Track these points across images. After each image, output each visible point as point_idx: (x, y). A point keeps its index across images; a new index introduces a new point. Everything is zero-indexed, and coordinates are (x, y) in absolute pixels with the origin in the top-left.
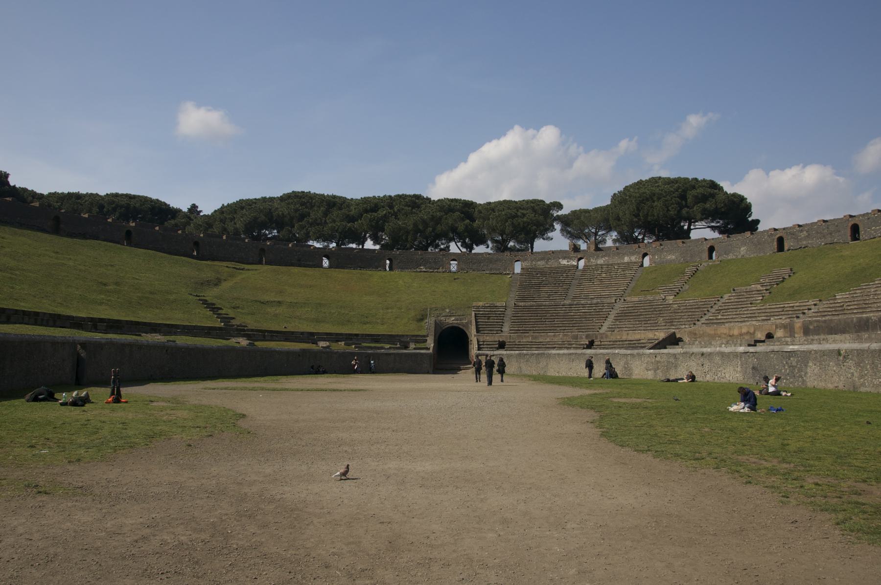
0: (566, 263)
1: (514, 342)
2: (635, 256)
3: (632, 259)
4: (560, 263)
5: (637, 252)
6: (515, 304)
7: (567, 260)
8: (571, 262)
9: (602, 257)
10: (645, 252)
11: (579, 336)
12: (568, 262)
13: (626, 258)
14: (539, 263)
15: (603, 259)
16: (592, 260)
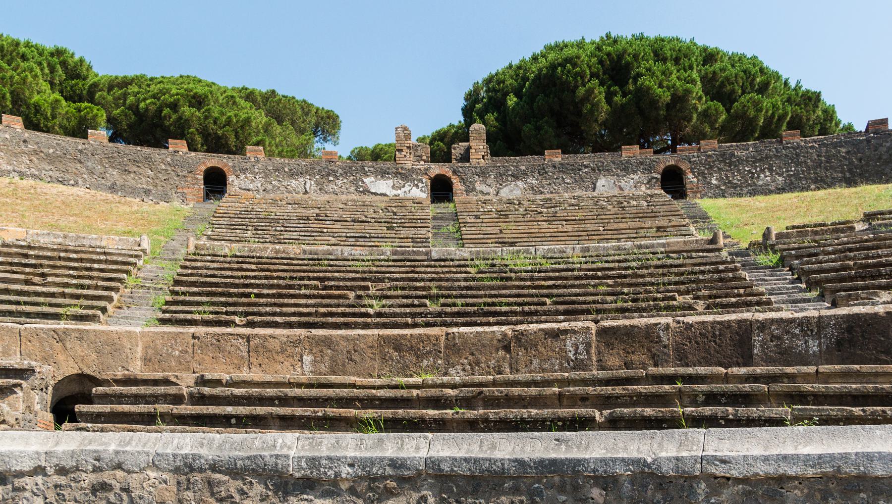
0: (391, 192)
1: (167, 382)
2: (636, 177)
3: (623, 184)
4: (366, 191)
5: (642, 163)
6: (196, 247)
7: (390, 182)
8: (407, 188)
9: (516, 177)
10: (672, 163)
11: (757, 339)
12: (393, 187)
13: (602, 182)
14: (293, 183)
15: (520, 183)
16: (479, 187)
